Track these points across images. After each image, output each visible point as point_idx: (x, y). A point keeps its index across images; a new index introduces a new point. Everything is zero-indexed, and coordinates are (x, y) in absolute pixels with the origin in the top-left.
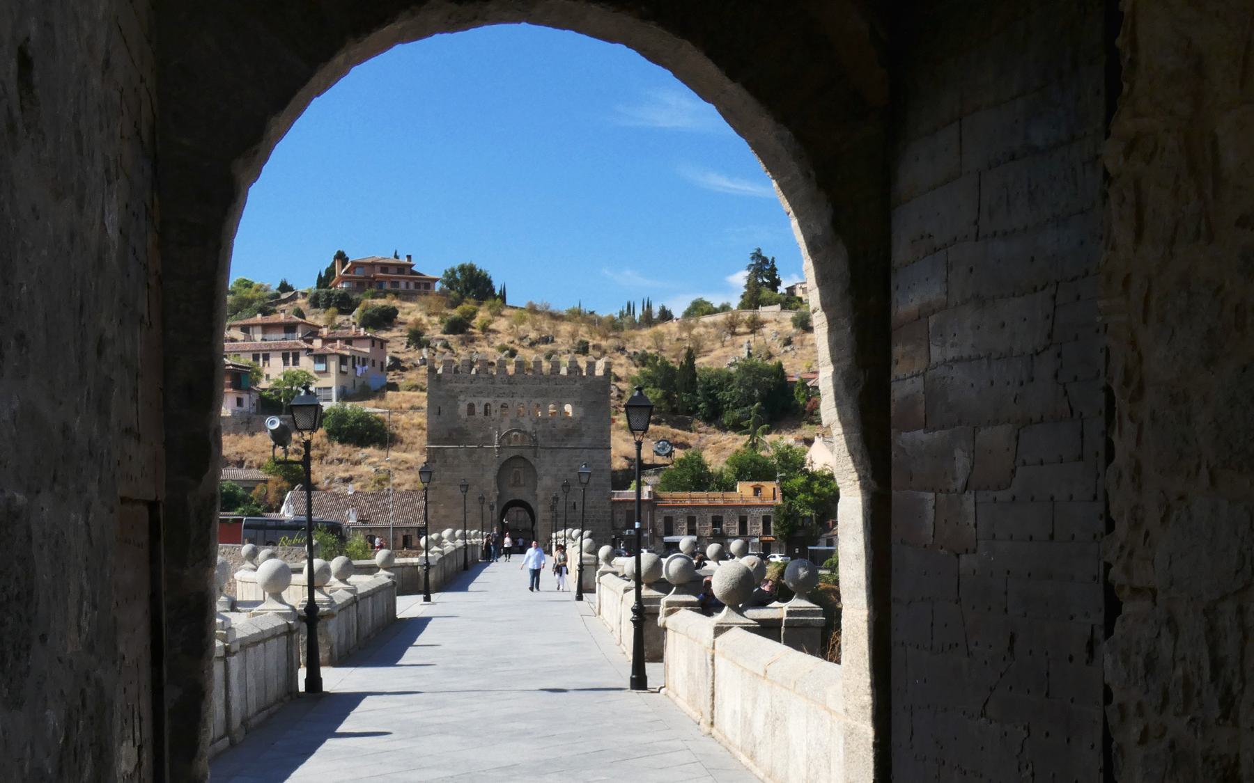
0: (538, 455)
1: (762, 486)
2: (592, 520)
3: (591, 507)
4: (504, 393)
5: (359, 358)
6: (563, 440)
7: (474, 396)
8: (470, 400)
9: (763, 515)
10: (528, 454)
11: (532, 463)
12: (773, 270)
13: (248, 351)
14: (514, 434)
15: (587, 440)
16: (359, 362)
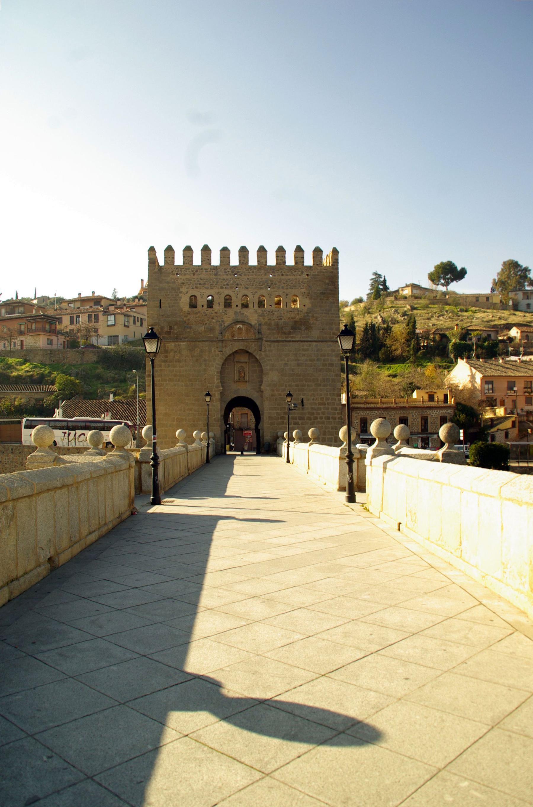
0: (263, 348)
1: (435, 393)
2: (321, 418)
3: (319, 404)
4: (227, 285)
5: (138, 318)
6: (290, 333)
7: (197, 288)
8: (192, 292)
9: (440, 415)
10: (253, 348)
11: (258, 357)
12: (385, 281)
13: (67, 314)
14: (238, 326)
15: (315, 334)
16: (138, 321)
